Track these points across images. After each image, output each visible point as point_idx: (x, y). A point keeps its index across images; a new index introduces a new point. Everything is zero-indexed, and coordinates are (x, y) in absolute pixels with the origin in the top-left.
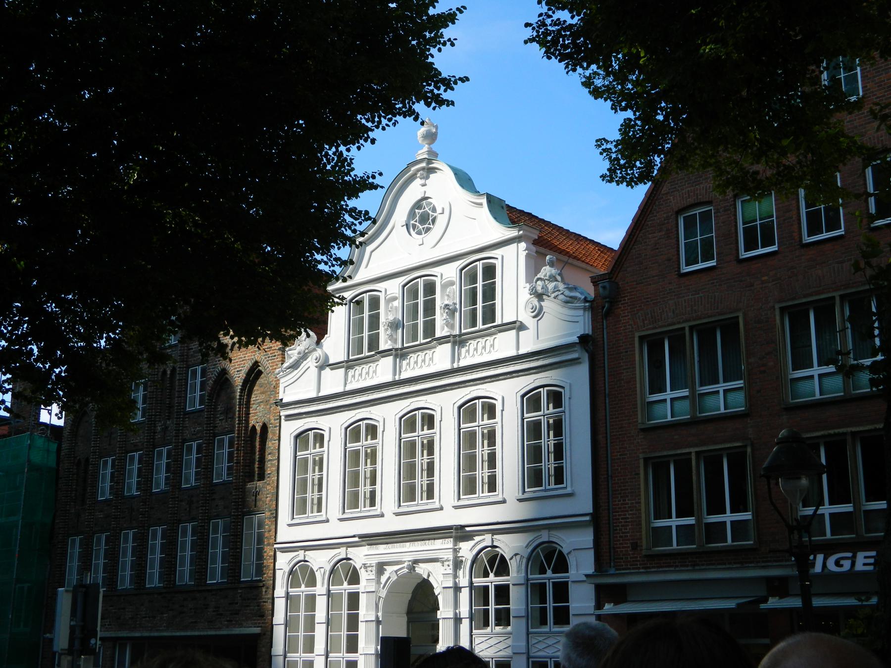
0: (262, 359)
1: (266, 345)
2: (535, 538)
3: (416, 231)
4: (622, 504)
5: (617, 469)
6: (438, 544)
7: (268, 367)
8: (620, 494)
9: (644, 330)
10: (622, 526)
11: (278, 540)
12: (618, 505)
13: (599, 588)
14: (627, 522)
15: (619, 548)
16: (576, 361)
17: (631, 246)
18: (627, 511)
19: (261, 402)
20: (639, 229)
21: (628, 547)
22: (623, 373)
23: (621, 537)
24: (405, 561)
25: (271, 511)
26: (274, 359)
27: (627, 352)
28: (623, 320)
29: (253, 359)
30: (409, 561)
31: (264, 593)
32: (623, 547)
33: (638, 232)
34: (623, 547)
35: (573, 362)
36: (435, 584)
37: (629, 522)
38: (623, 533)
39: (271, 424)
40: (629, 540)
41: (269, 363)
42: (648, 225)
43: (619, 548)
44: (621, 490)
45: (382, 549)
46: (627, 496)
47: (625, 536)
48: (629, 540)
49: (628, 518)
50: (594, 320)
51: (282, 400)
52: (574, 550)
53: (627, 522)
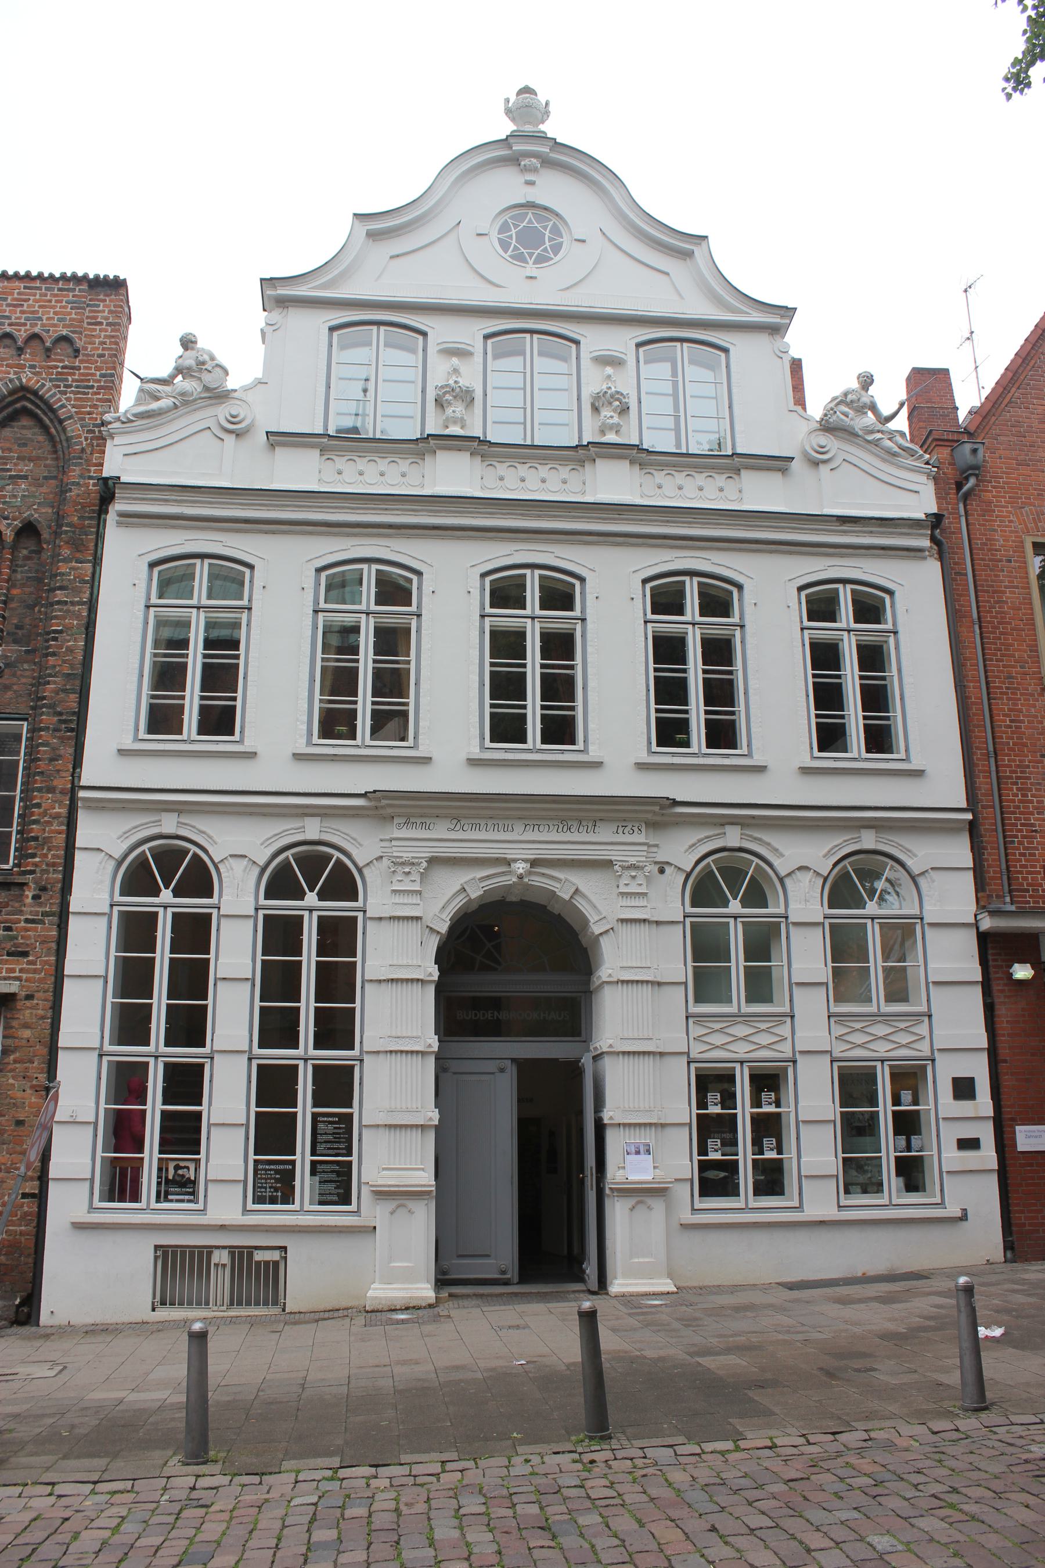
0: (43, 385)
1: (62, 361)
2: (845, 841)
3: (509, 253)
4: (1020, 801)
5: (1008, 743)
6: (605, 833)
7: (63, 406)
8: (1016, 783)
9: (1038, 535)
10: (1023, 837)
11: (83, 783)
12: (1013, 801)
13: (984, 939)
14: (1033, 831)
15: (1021, 873)
16: (919, 554)
17: (1003, 406)
18: (1032, 814)
19: (25, 477)
20: (1017, 385)
21: (1039, 873)
22: (1005, 592)
23: (1021, 854)
24: (515, 860)
25: (60, 714)
26: (88, 393)
27: (1009, 561)
28: (998, 511)
29: (11, 381)
30: (525, 861)
31: (29, 900)
32: (1029, 873)
33: (1014, 389)
34: (1029, 873)
35: (912, 554)
36: (592, 917)
37: (1036, 831)
38: (1025, 848)
39: (68, 525)
40: (1038, 861)
41: (68, 399)
42: (1029, 385)
43: (1021, 873)
44: (1018, 778)
45: (441, 830)
46: (1030, 790)
47: (1031, 855)
48: (1038, 861)
49: (1033, 825)
50: (940, 497)
51: (119, 478)
52: (932, 869)
53: (1033, 831)
